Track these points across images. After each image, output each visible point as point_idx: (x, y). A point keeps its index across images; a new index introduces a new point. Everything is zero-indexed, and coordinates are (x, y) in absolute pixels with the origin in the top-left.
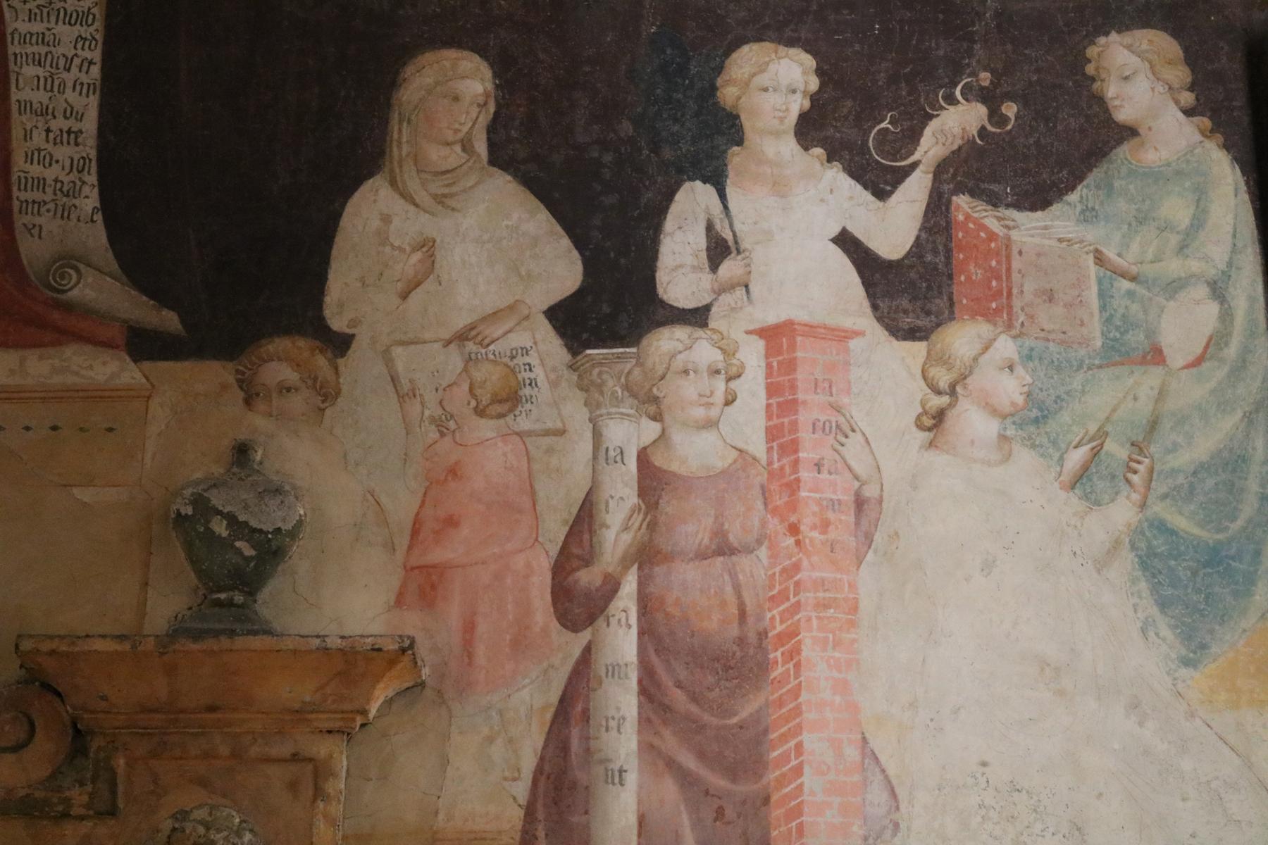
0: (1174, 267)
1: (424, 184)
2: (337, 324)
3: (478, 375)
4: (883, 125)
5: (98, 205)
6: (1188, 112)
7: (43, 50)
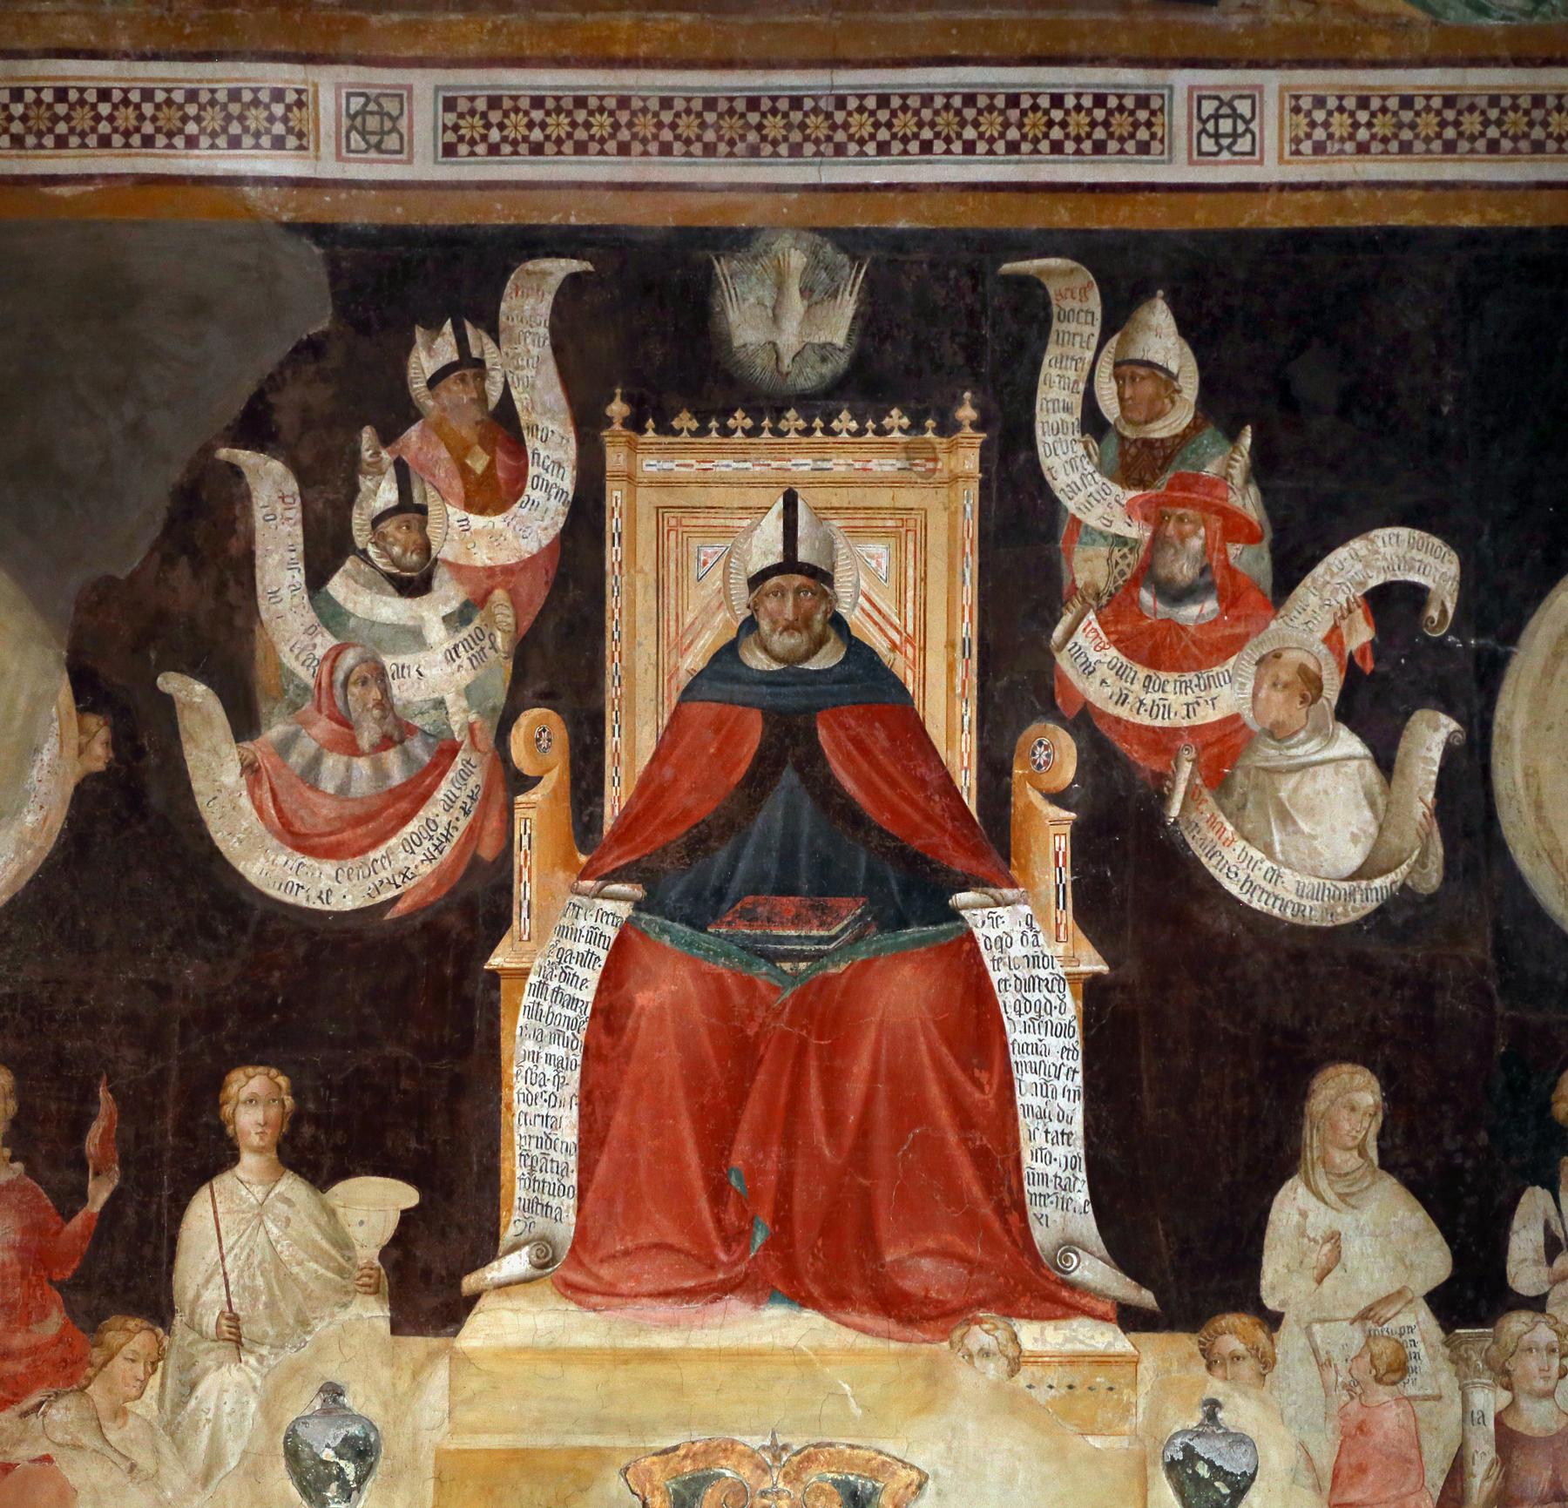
1: (1331, 1184)
2: (1271, 1303)
3: (1376, 1349)
7: (1037, 1059)
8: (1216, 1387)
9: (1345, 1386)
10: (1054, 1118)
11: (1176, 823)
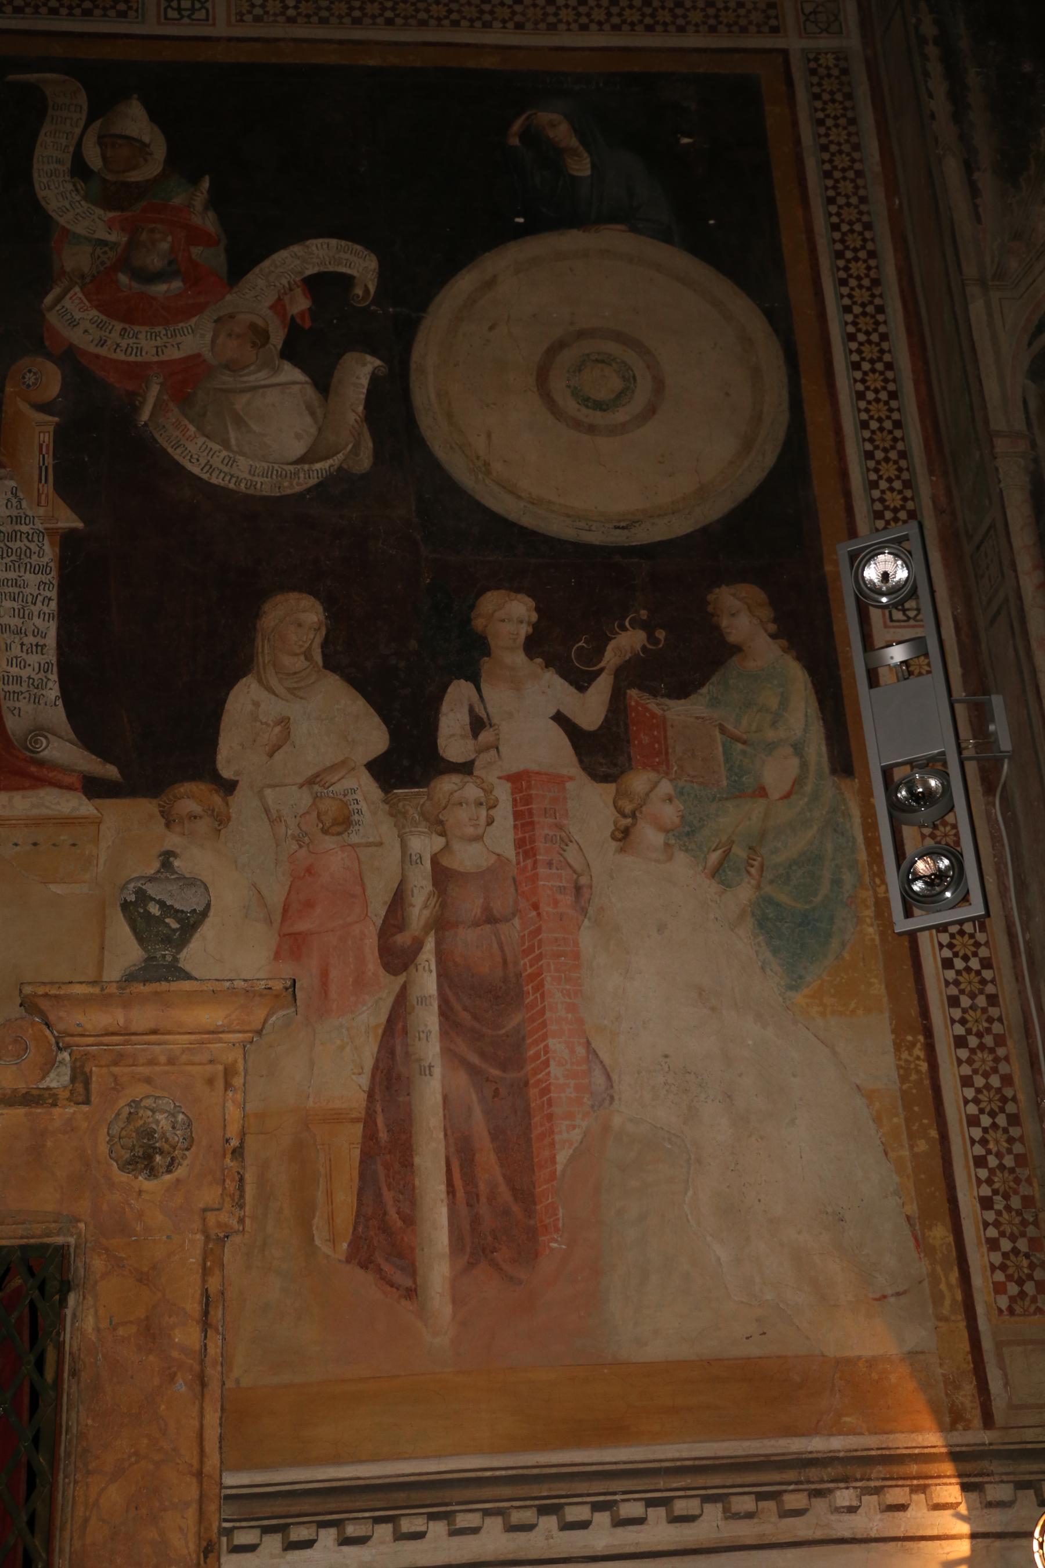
0: (770, 735)
2: (226, 773)
4: (580, 644)
5: (59, 694)
6: (773, 636)
7: (16, 590)
8: (173, 841)
9: (294, 837)
10: (30, 634)
11: (146, 425)
